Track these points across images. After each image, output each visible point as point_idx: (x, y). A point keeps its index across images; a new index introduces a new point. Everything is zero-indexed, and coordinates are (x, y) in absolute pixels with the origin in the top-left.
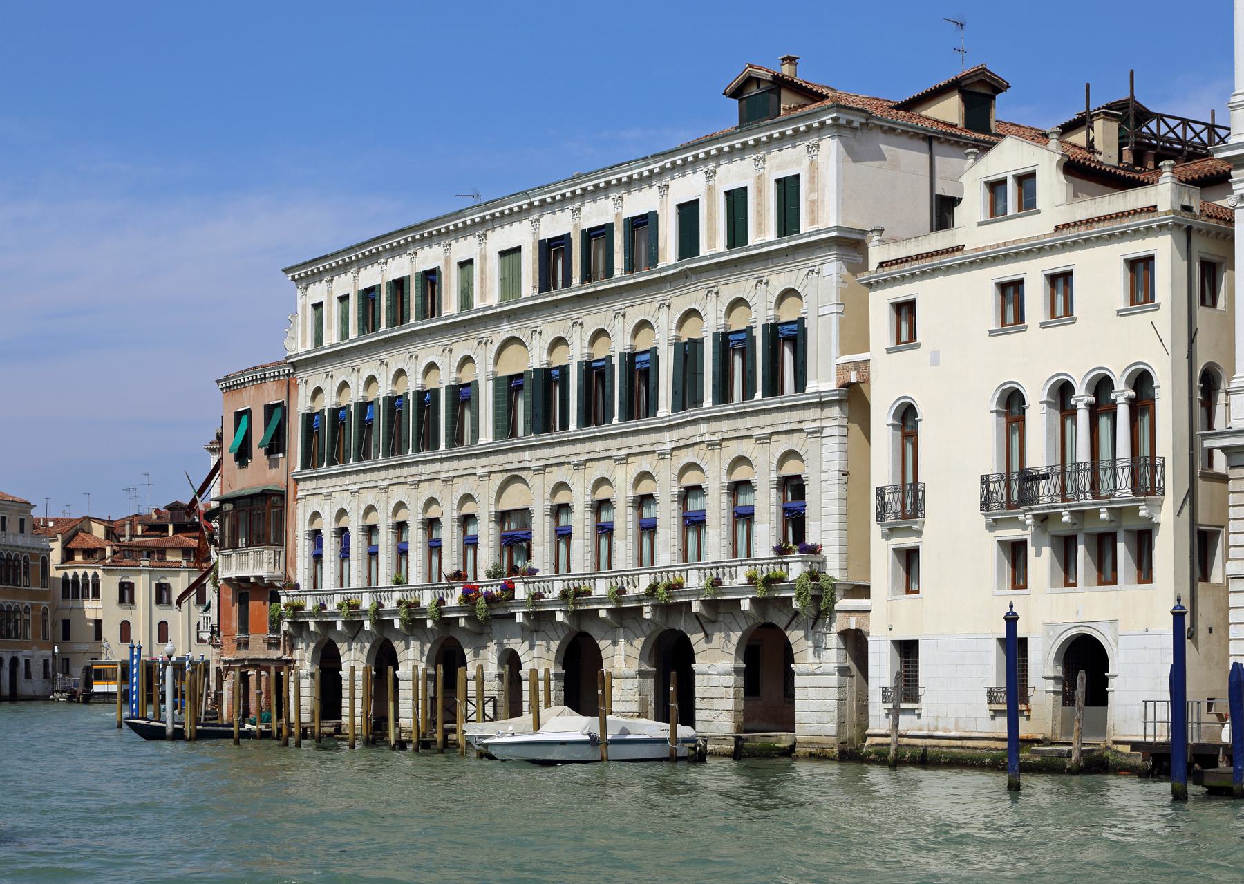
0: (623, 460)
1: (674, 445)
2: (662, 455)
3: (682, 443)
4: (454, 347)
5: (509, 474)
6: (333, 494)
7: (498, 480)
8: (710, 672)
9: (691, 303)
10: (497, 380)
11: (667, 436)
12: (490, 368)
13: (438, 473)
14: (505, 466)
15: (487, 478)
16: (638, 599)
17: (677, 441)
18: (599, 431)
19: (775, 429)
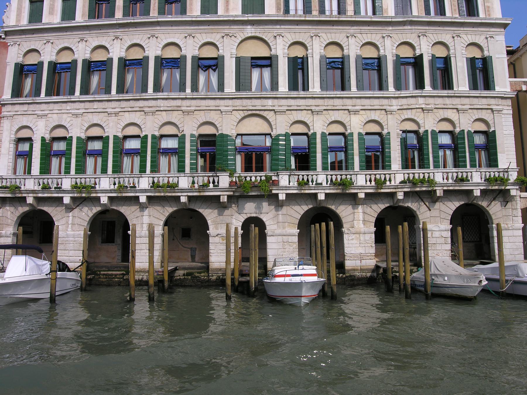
0: (356, 112)
1: (399, 108)
2: (391, 112)
3: (405, 107)
4: (197, 35)
5: (250, 112)
6: (49, 115)
7: (240, 115)
8: (433, 229)
9: (407, 39)
10: (238, 60)
11: (394, 102)
12: (234, 51)
13: (180, 107)
14: (247, 107)
15: (230, 113)
16: (396, 187)
17: (402, 105)
18: (340, 94)
19: (472, 107)
